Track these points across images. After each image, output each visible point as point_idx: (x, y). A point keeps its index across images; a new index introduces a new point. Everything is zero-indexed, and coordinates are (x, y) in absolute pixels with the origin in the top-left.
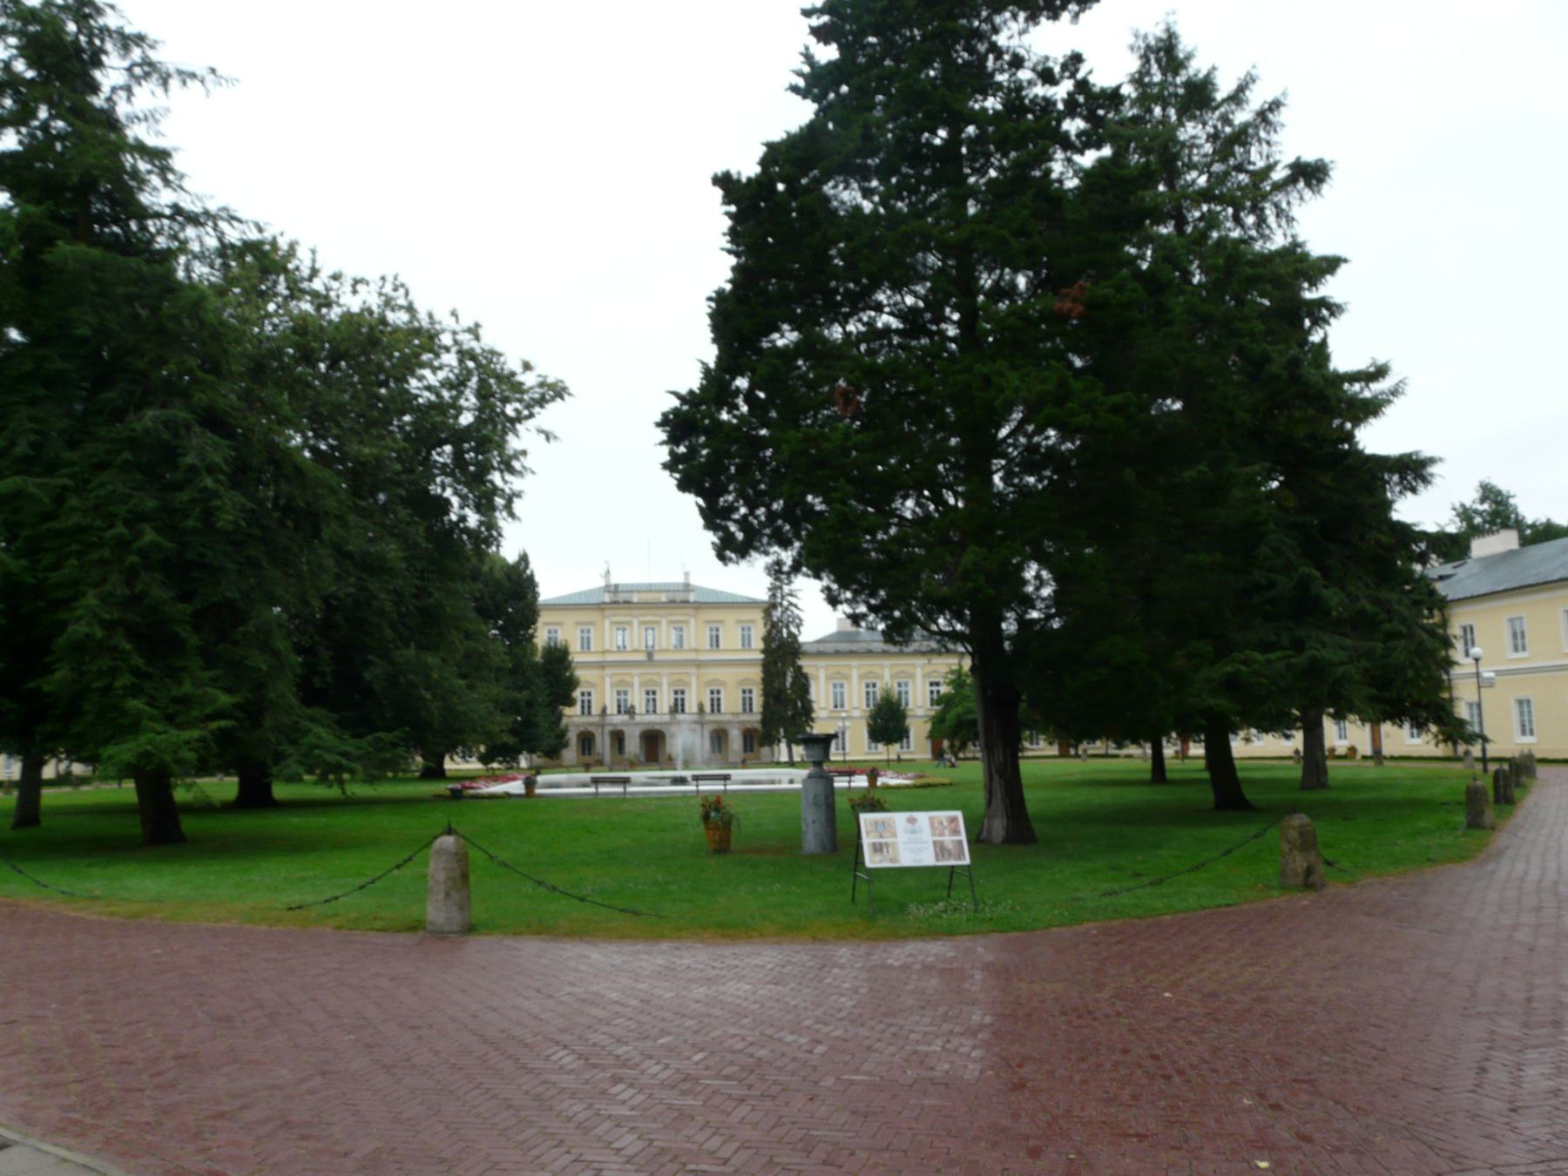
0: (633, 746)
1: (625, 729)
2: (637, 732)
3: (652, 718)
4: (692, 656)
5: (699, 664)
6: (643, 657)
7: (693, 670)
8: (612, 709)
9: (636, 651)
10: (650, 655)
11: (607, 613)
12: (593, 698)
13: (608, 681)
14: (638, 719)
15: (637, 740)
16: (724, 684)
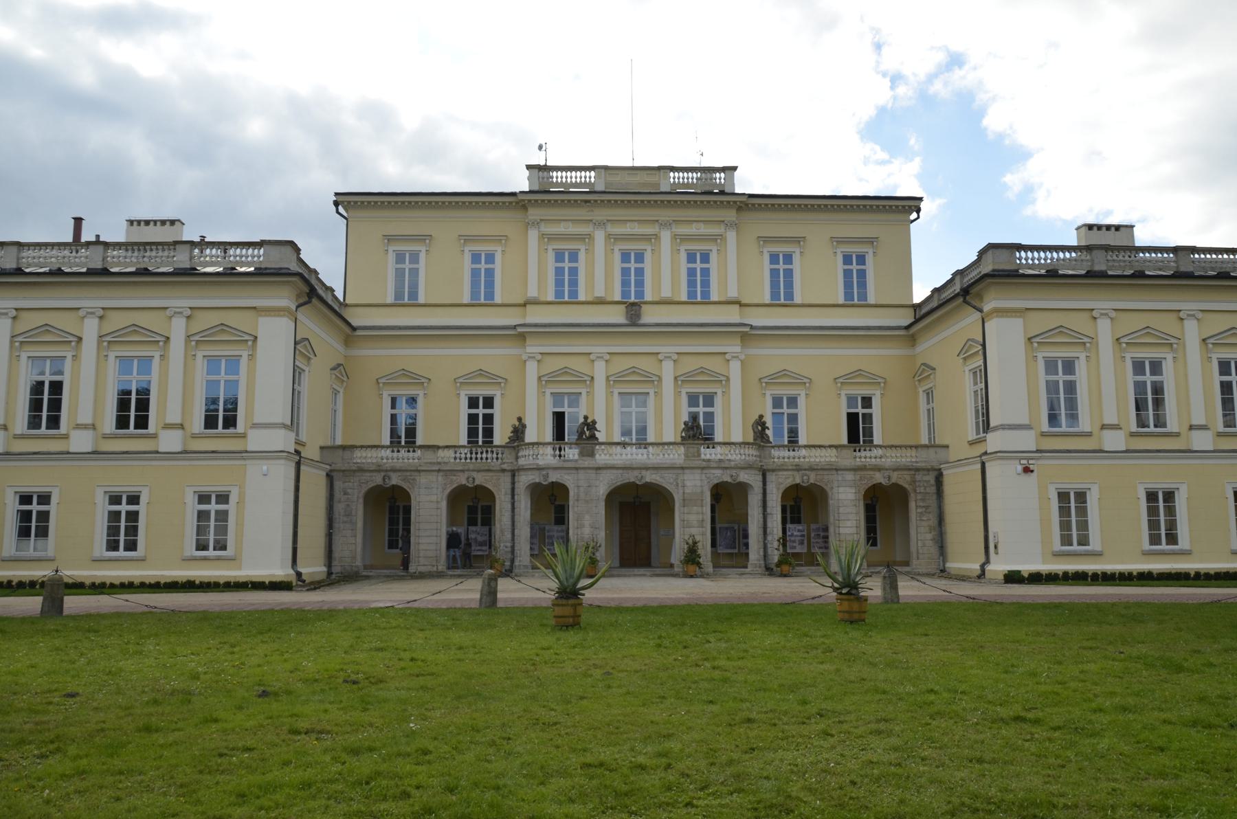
0: (589, 521)
1: (568, 480)
2: (602, 490)
3: (633, 455)
4: (732, 315)
5: (748, 335)
6: (616, 315)
7: (734, 347)
8: (539, 429)
9: (600, 302)
10: (634, 310)
11: (534, 213)
12: (497, 411)
13: (532, 369)
14: (602, 456)
15: (601, 509)
16: (804, 382)
